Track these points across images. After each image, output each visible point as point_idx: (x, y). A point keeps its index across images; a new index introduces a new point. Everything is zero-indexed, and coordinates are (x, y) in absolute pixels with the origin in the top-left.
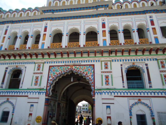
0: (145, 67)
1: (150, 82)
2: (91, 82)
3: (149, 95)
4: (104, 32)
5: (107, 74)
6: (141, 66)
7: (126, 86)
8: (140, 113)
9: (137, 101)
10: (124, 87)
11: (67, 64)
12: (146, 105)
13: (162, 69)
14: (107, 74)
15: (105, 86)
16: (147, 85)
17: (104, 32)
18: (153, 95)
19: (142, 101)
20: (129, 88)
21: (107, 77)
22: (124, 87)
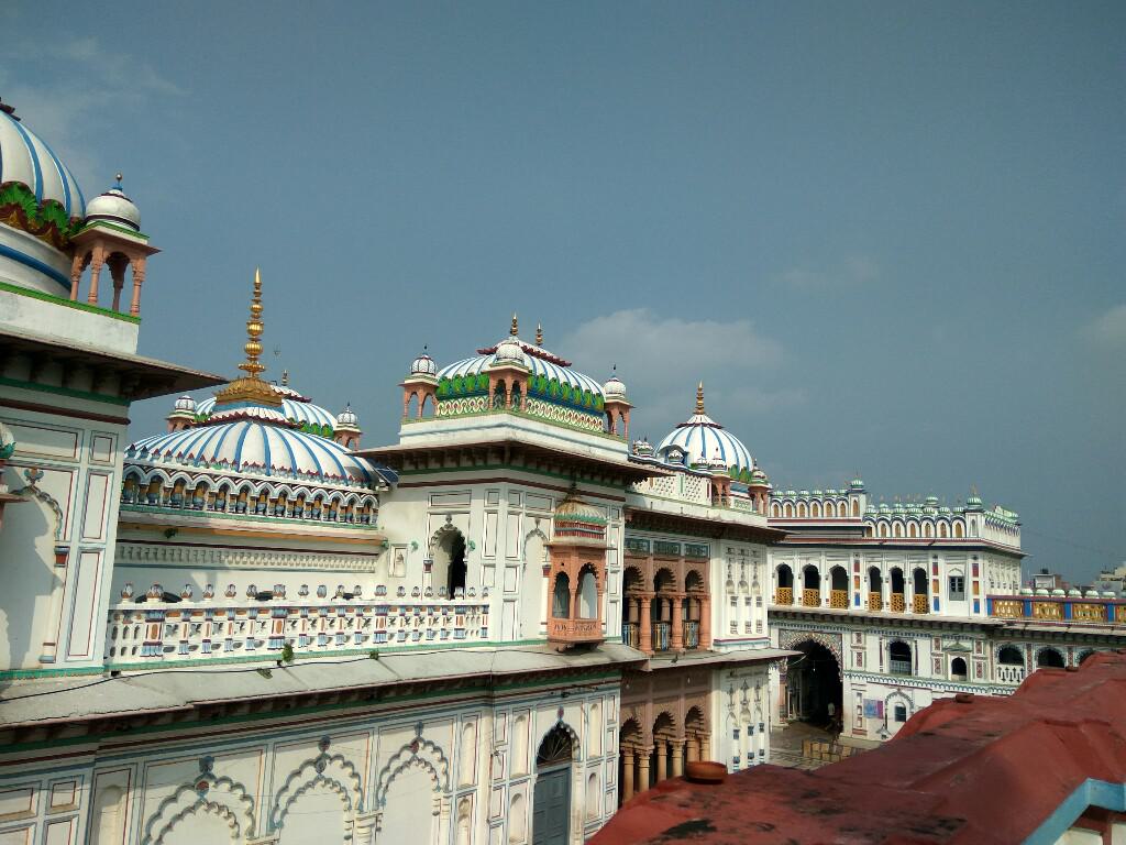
0: (914, 644)
1: (916, 669)
2: (837, 659)
3: (911, 685)
4: (857, 578)
5: (859, 651)
6: (909, 643)
7: (886, 670)
8: (900, 705)
9: (895, 690)
10: (881, 670)
11: (803, 629)
12: (907, 697)
13: (934, 651)
14: (859, 651)
15: (855, 668)
16: (914, 672)
17: (857, 578)
18: (915, 685)
19: (903, 691)
20: (893, 672)
21: (859, 654)
22: (881, 670)
